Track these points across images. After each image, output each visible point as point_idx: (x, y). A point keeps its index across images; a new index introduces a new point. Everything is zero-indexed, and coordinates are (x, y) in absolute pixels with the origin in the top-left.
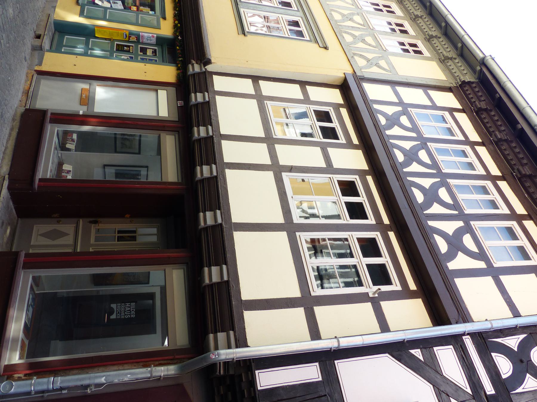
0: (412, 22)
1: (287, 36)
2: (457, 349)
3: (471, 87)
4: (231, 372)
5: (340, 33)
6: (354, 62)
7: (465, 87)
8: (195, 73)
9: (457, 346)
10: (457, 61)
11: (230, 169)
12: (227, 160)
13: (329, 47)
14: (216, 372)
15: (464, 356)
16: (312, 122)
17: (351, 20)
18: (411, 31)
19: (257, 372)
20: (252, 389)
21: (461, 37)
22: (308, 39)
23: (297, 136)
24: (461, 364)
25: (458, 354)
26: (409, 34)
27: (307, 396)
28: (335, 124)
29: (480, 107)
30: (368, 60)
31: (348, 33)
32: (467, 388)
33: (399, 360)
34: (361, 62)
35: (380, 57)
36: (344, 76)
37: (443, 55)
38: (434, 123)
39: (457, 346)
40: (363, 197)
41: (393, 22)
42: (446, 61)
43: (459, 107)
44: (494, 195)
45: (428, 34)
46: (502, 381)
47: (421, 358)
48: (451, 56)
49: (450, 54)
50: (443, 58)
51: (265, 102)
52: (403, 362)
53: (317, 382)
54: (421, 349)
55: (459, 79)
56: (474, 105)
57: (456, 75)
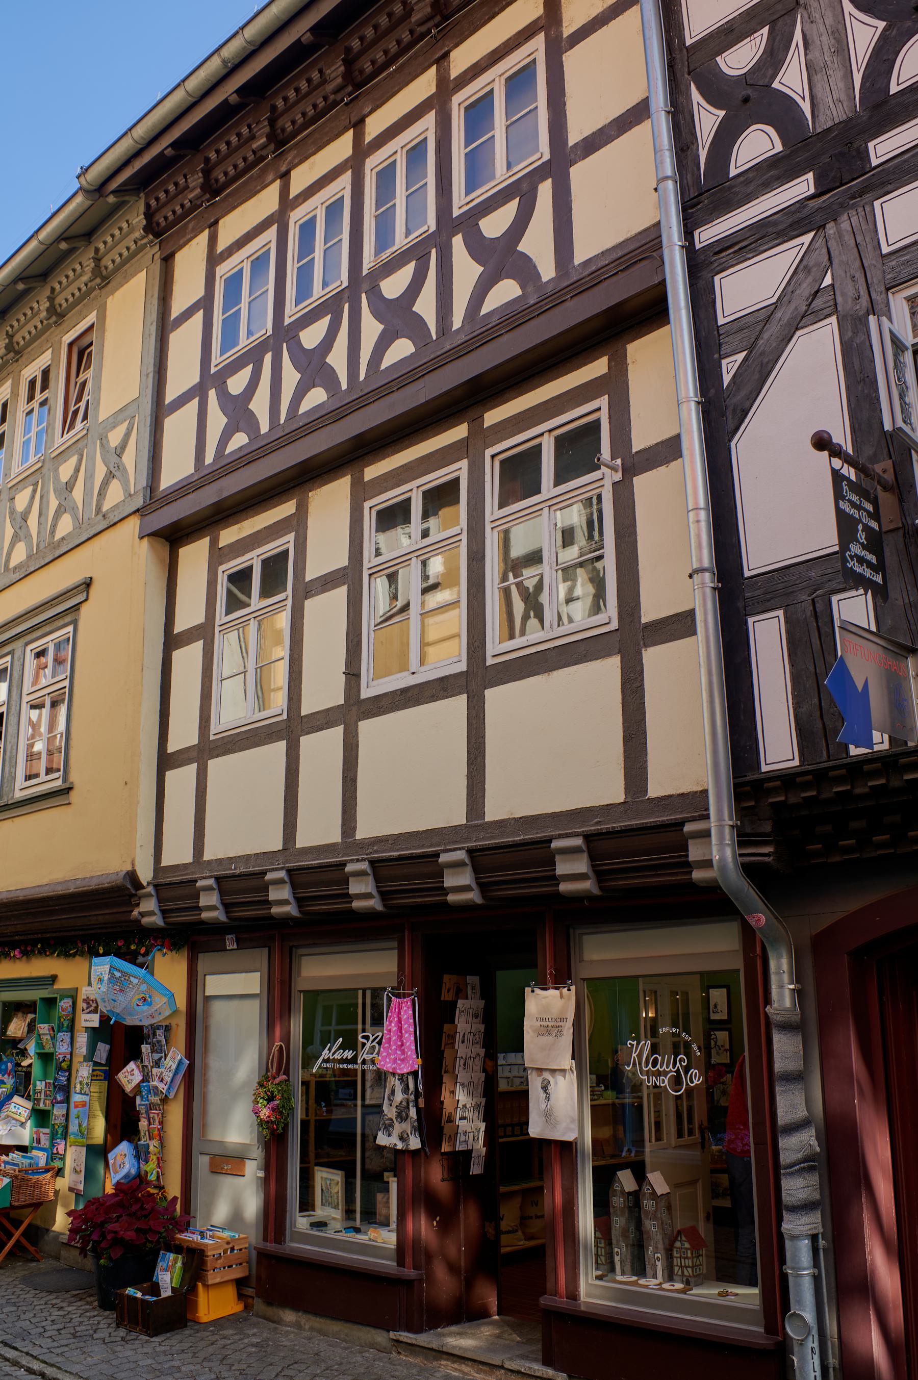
0: (23, 359)
1: (66, 683)
2: (723, 265)
3: (158, 209)
4: (767, 827)
5: (54, 548)
6: (116, 513)
7: (158, 224)
8: (160, 910)
9: (716, 265)
10: (101, 246)
11: (355, 829)
12: (335, 836)
13: (86, 578)
14: (766, 864)
15: (737, 248)
16: (252, 620)
17: (25, 517)
18: (45, 359)
19: (764, 768)
20: (798, 780)
21: (44, 247)
22: (70, 628)
23: (283, 658)
24: (753, 257)
25: (732, 262)
26: (49, 365)
27: (814, 646)
28: (255, 558)
29: (201, 188)
30: (110, 476)
31: (54, 526)
32: (803, 244)
33: (745, 413)
34: (115, 494)
35: (102, 445)
36: (146, 540)
37: (91, 281)
38: (242, 305)
40: (412, 490)
41: (26, 407)
42: (104, 273)
43: (204, 236)
44: (395, 150)
45: (48, 319)
46: (788, 152)
47: (740, 357)
48: (92, 260)
49: (88, 263)
50: (98, 280)
51: (212, 738)
52: (748, 403)
53: (786, 622)
54: (721, 358)
55: (140, 240)
56: (199, 202)
57: (133, 247)
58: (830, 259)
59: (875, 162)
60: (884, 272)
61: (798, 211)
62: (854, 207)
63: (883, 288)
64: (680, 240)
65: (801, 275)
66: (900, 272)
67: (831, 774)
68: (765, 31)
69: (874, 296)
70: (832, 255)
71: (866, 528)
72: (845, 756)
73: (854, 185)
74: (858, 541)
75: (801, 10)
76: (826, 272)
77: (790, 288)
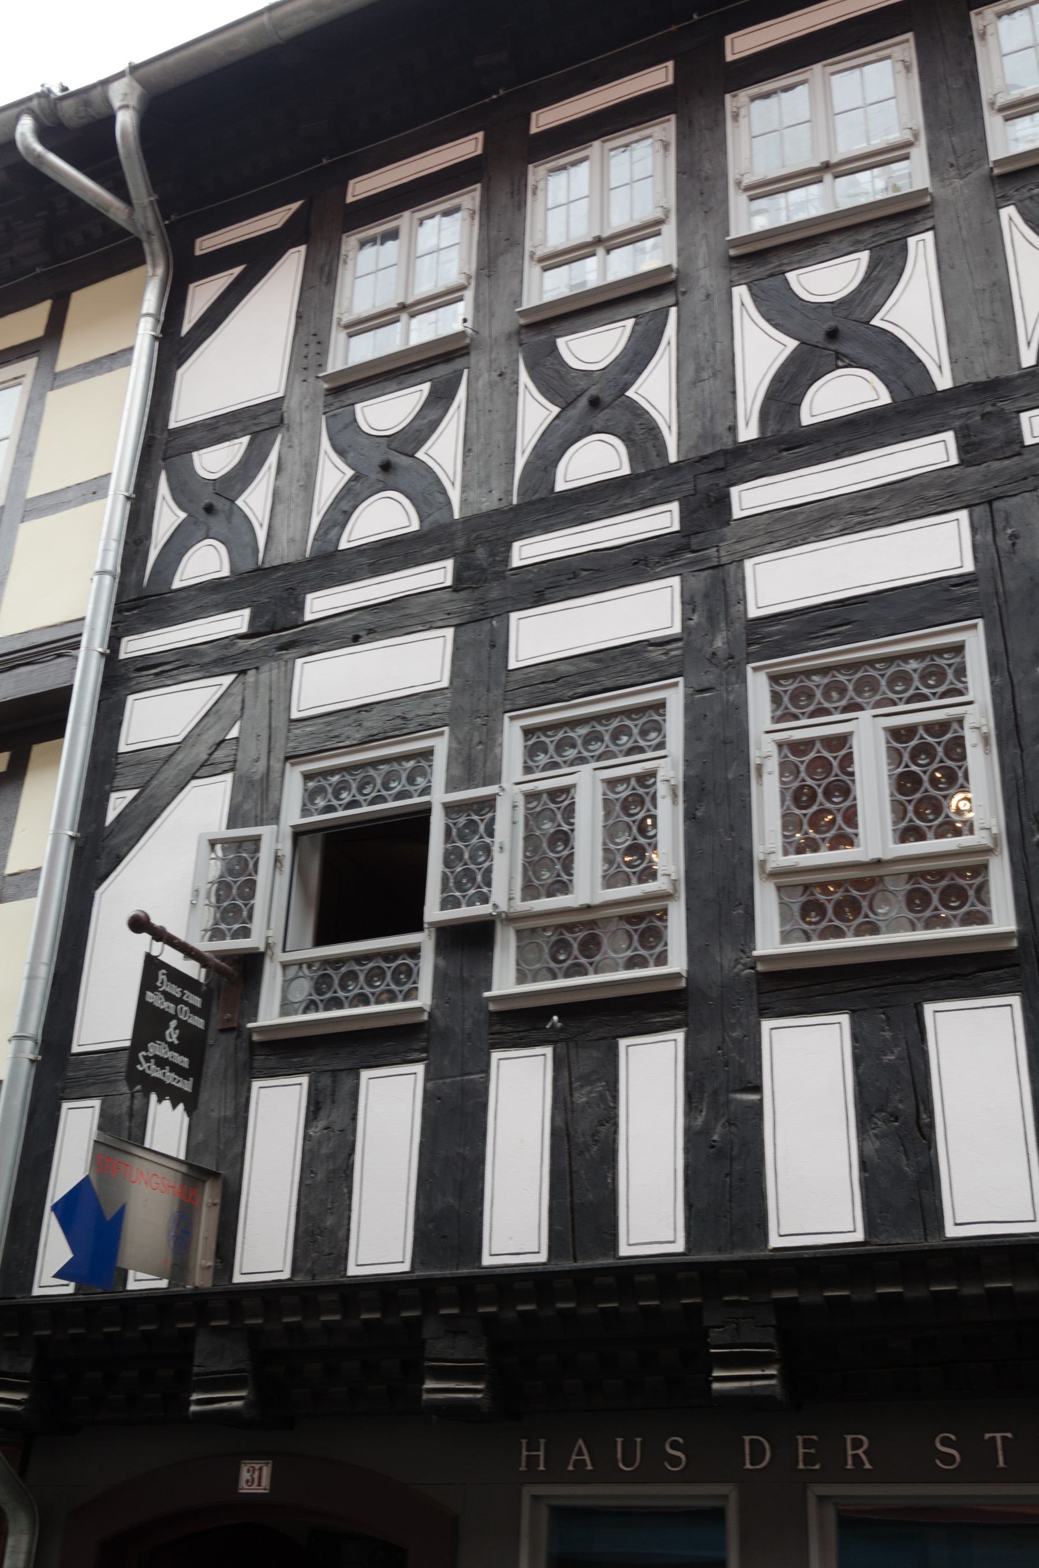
4: (27, 1366)
9: (134, 682)
33: (119, 859)
39: (134, 682)
46: (232, 579)
47: (131, 794)
52: (125, 849)
58: (242, 709)
59: (308, 616)
60: (287, 738)
61: (226, 647)
62: (277, 659)
63: (282, 757)
64: (102, 646)
65: (210, 720)
66: (300, 743)
68: (245, 440)
69: (272, 763)
70: (246, 706)
71: (182, 1025)
72: (121, 1289)
73: (284, 635)
74: (163, 1039)
75: (284, 430)
76: (235, 722)
77: (197, 731)
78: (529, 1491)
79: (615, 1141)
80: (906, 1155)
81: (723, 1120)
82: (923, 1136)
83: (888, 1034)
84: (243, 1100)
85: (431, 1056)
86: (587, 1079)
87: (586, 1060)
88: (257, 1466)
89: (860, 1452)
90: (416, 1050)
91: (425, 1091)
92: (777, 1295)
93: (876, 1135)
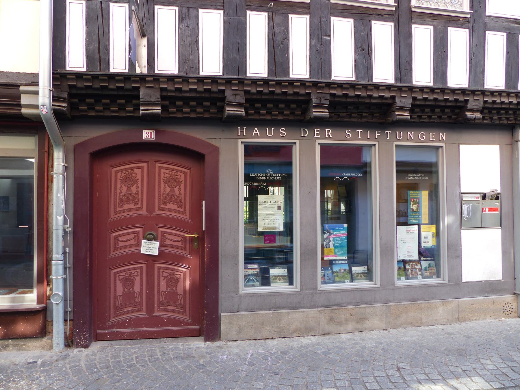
4: (65, 95)
14: (63, 110)
20: (84, 77)
53: (86, 8)
67: (100, 77)
72: (108, 71)
78: (241, 140)
79: (288, 45)
80: (365, 61)
81: (320, 43)
82: (369, 55)
83: (362, 27)
84: (152, 12)
85: (225, 8)
86: (279, 25)
87: (278, 19)
88: (149, 132)
89: (329, 133)
90: (219, 6)
91: (224, 20)
92: (332, 92)
93: (358, 54)
